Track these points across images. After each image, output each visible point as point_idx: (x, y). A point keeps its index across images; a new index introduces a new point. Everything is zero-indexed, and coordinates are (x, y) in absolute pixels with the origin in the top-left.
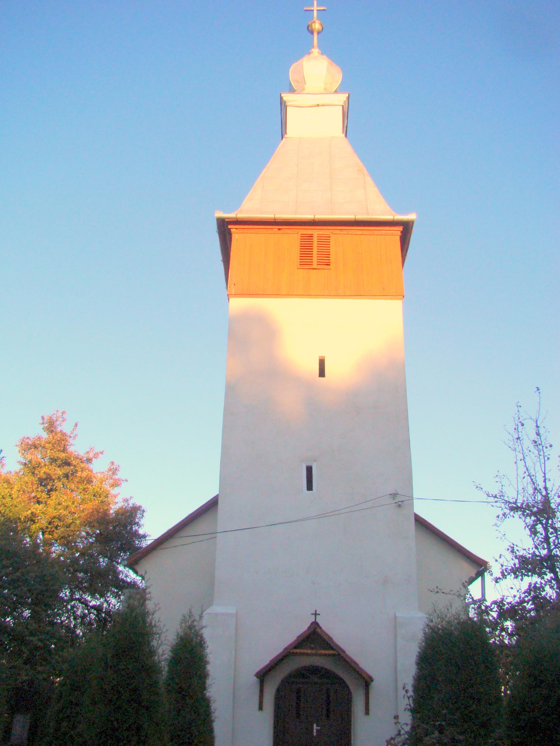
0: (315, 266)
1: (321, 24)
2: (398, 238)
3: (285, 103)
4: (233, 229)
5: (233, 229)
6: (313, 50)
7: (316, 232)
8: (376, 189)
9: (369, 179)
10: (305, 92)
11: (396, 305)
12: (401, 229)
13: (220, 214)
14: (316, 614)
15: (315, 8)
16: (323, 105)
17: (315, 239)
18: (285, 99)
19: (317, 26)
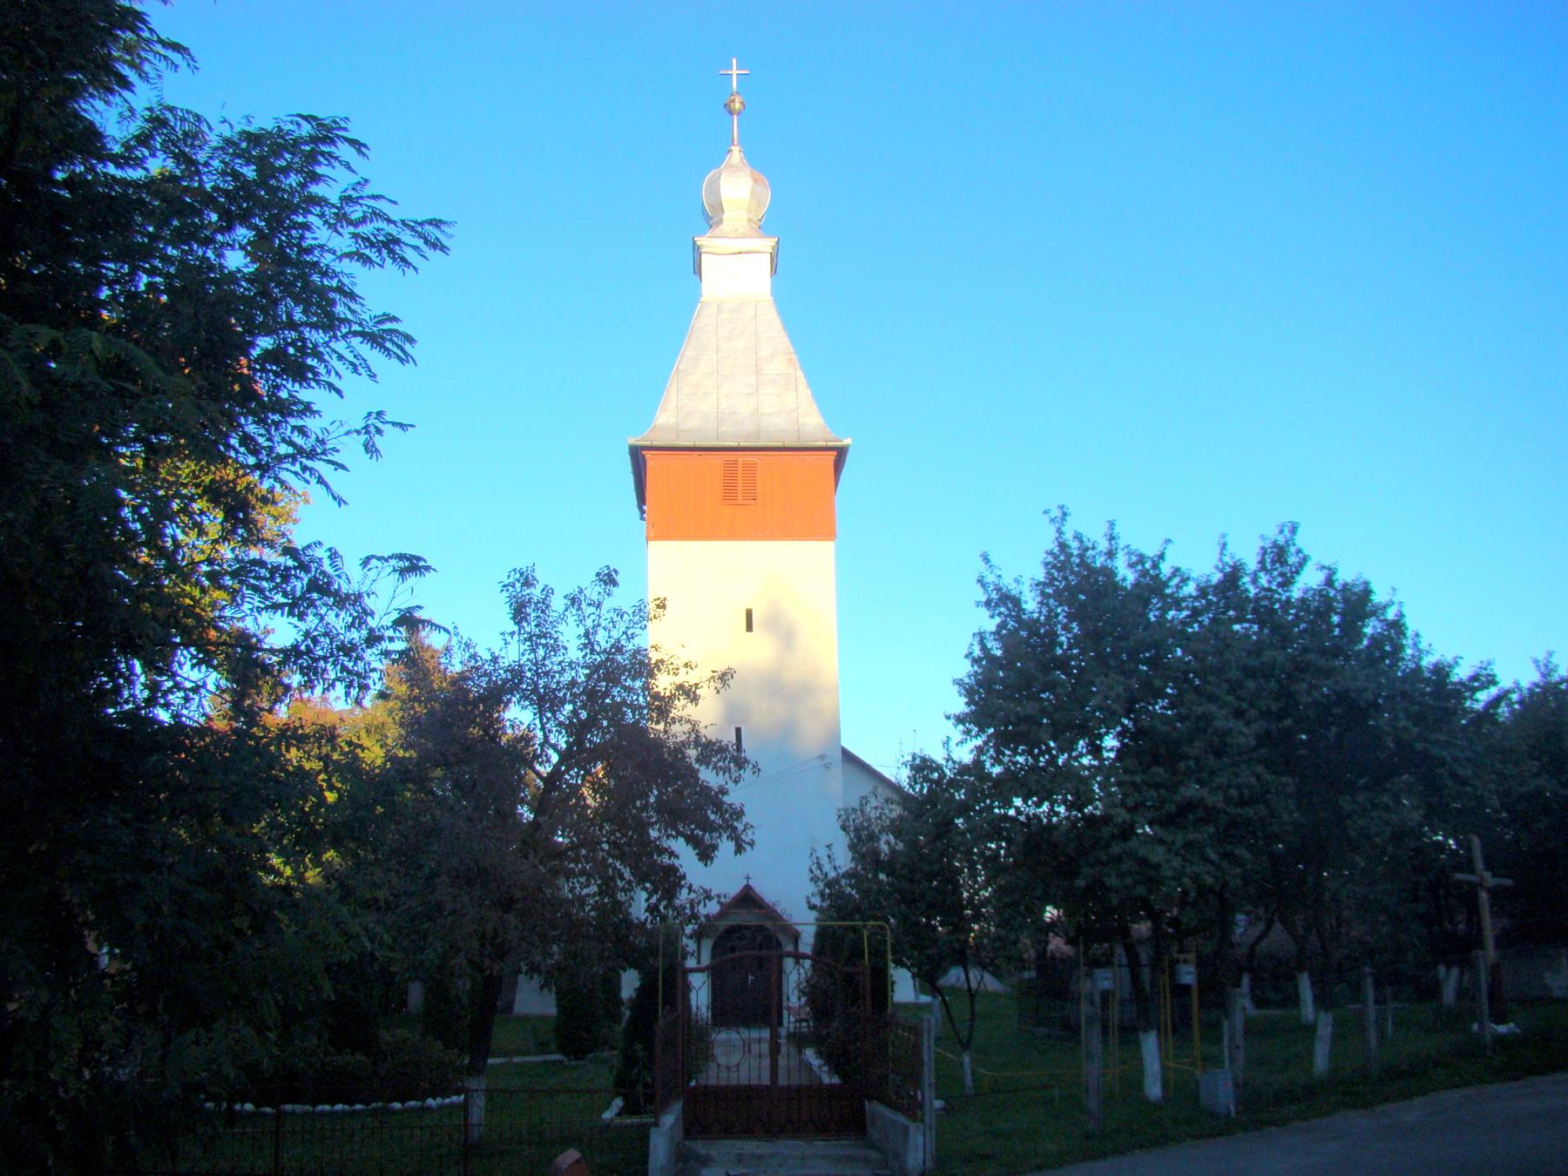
0: (740, 502)
1: (742, 103)
2: (832, 463)
3: (699, 248)
4: (648, 454)
5: (648, 454)
6: (733, 148)
7: (742, 458)
8: (808, 391)
9: (800, 373)
10: (725, 227)
11: (829, 546)
12: (835, 453)
13: (633, 441)
14: (748, 878)
15: (735, 72)
16: (747, 253)
17: (740, 465)
18: (698, 243)
19: (737, 106)
